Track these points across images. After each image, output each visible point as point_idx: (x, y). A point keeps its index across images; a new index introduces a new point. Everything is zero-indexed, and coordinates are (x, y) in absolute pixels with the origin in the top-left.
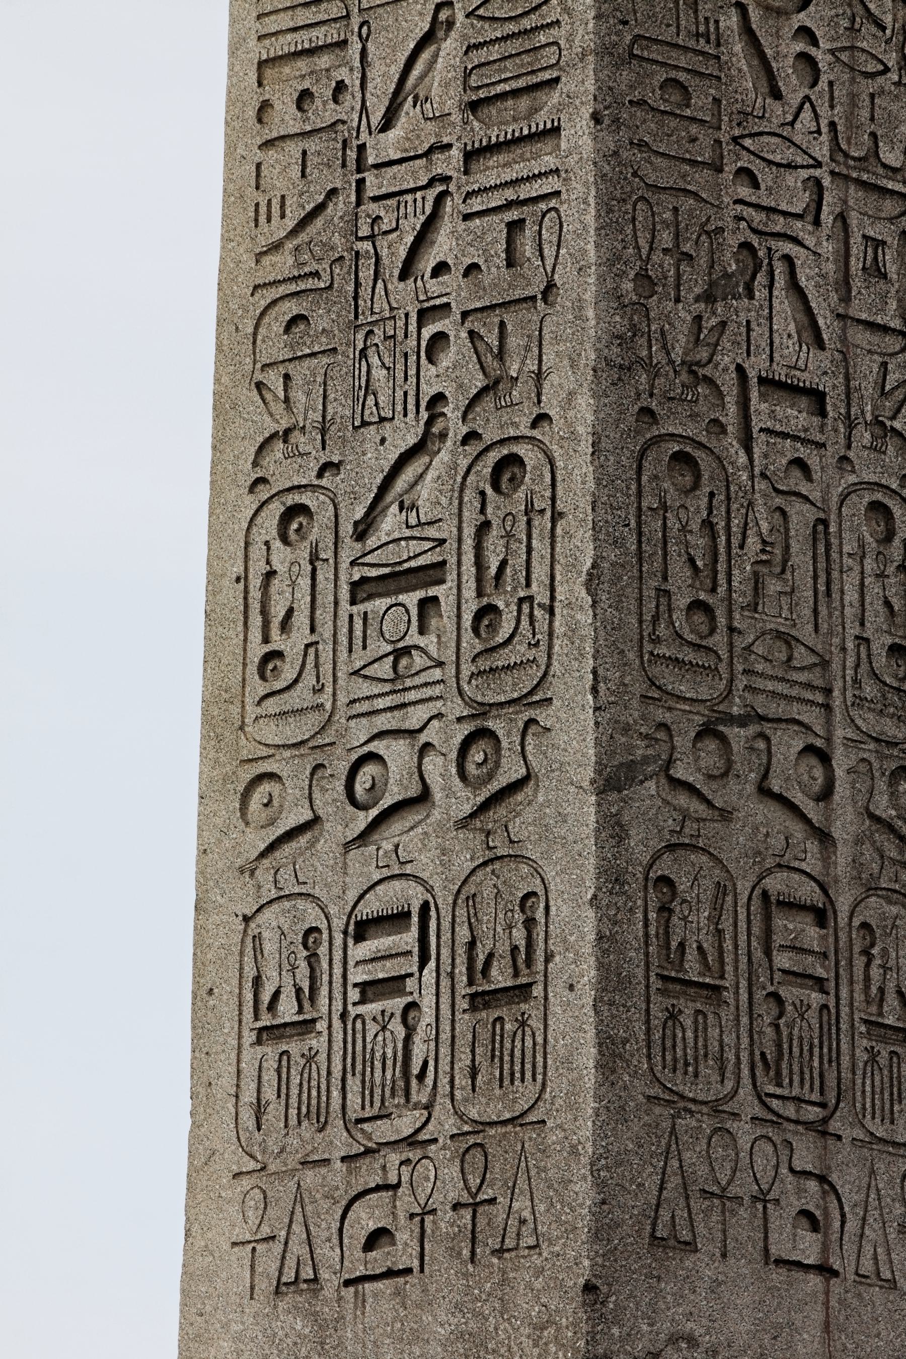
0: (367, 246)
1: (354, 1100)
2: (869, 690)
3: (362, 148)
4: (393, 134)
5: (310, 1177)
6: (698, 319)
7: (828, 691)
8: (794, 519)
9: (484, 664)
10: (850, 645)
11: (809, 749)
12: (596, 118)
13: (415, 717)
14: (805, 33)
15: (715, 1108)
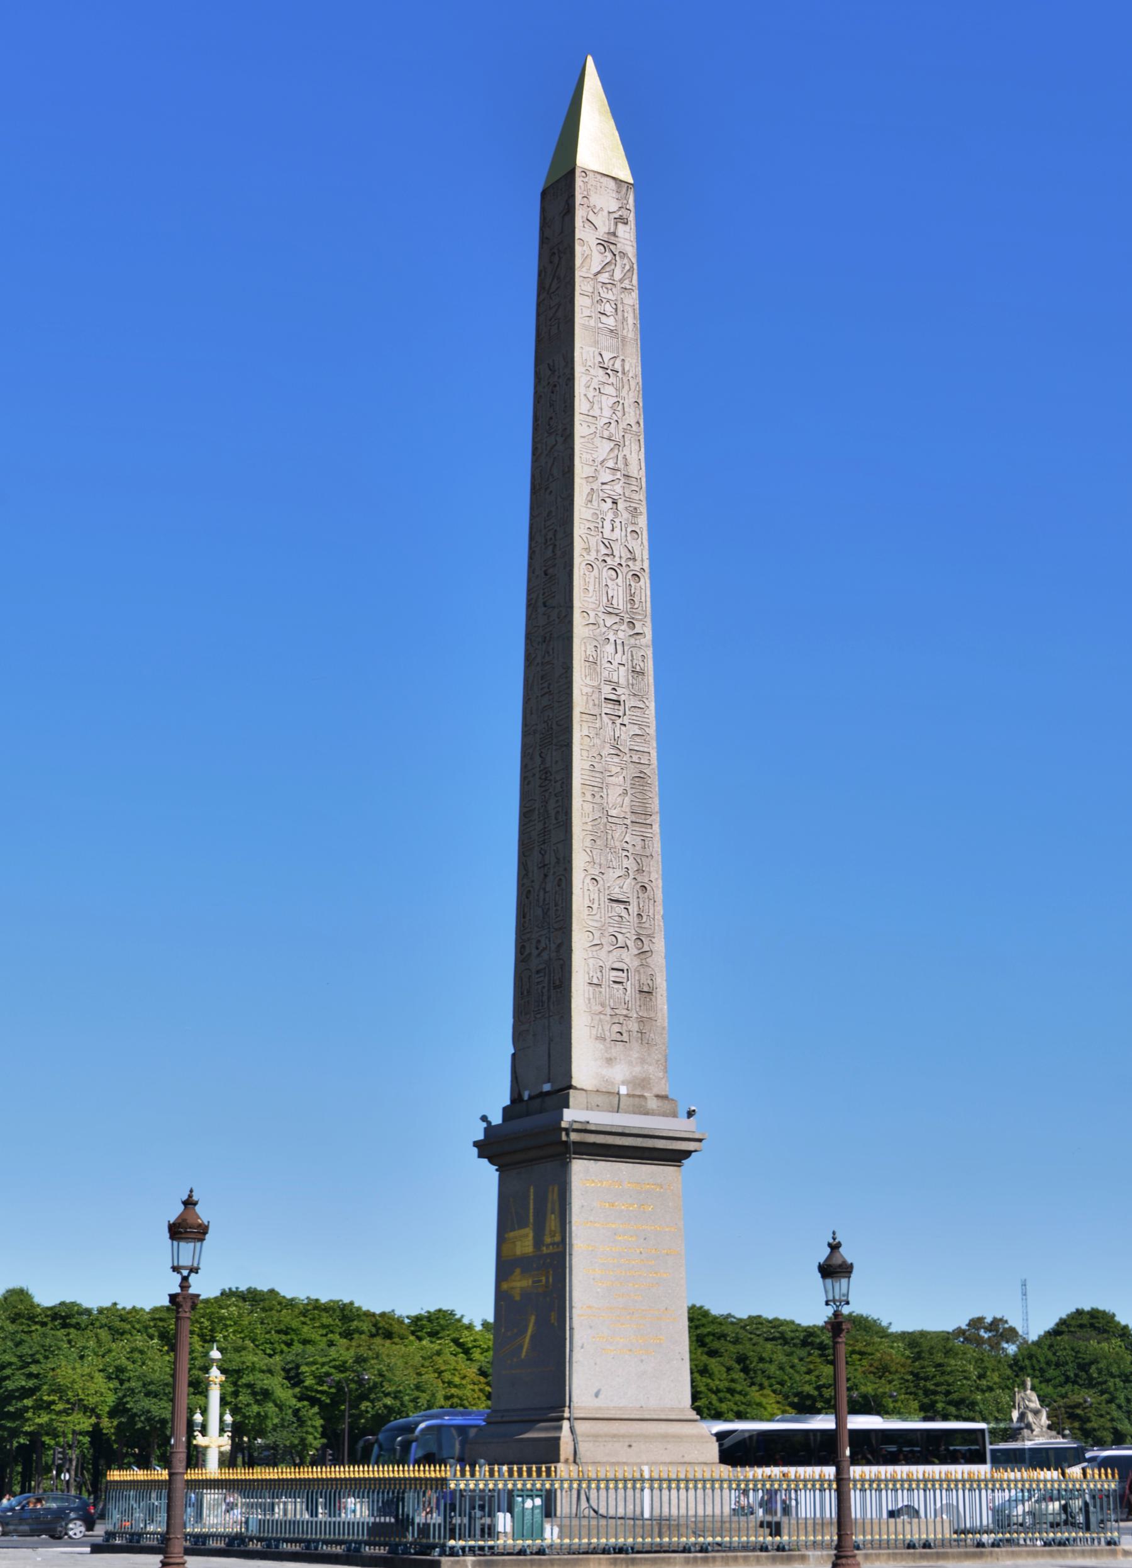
1: (612, 1005)
4: (615, 811)
5: (602, 1016)
13: (624, 931)
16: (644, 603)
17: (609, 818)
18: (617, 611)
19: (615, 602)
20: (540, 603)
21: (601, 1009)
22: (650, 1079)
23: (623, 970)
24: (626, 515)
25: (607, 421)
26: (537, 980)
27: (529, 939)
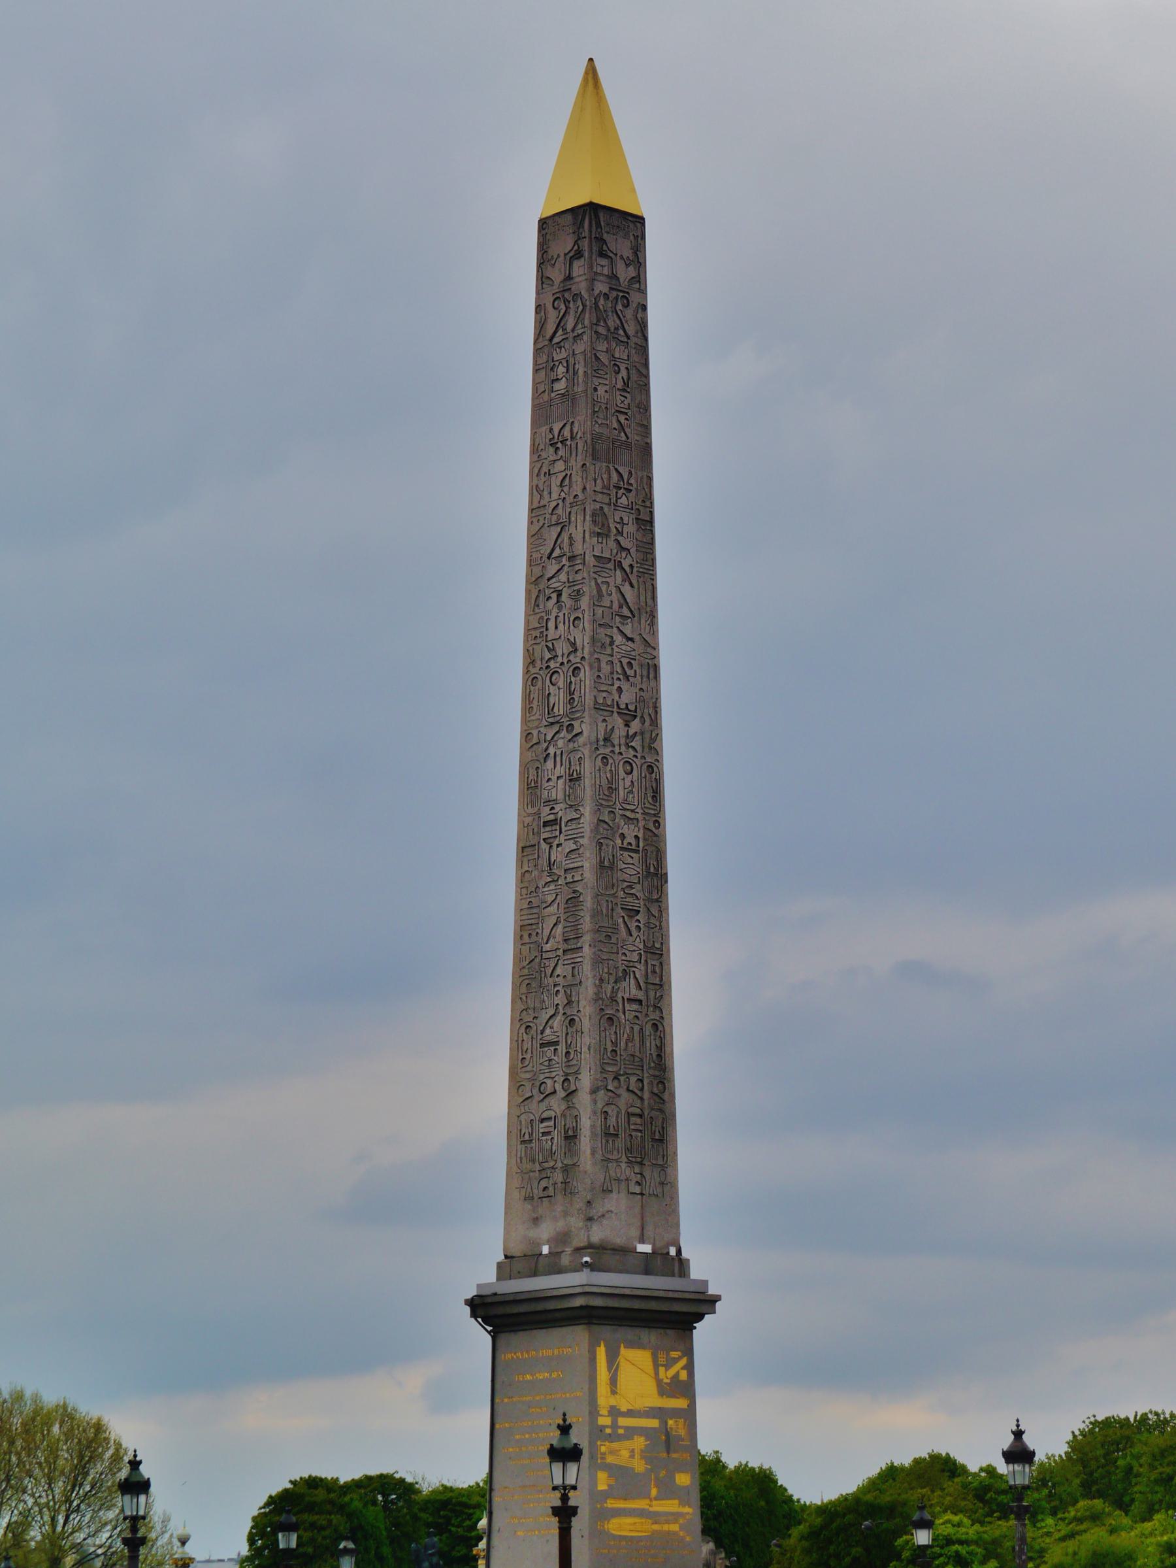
0: (543, 969)
1: (541, 1158)
2: (652, 1065)
3: (542, 947)
4: (548, 945)
5: (532, 1174)
6: (613, 987)
7: (643, 1066)
8: (635, 1029)
9: (567, 1064)
10: (648, 1055)
11: (638, 1079)
12: (590, 945)
13: (554, 1074)
14: (638, 921)
15: (617, 1161)
16: (583, 697)
19: (556, 709)
21: (529, 1166)
22: (571, 1231)
23: (549, 1119)
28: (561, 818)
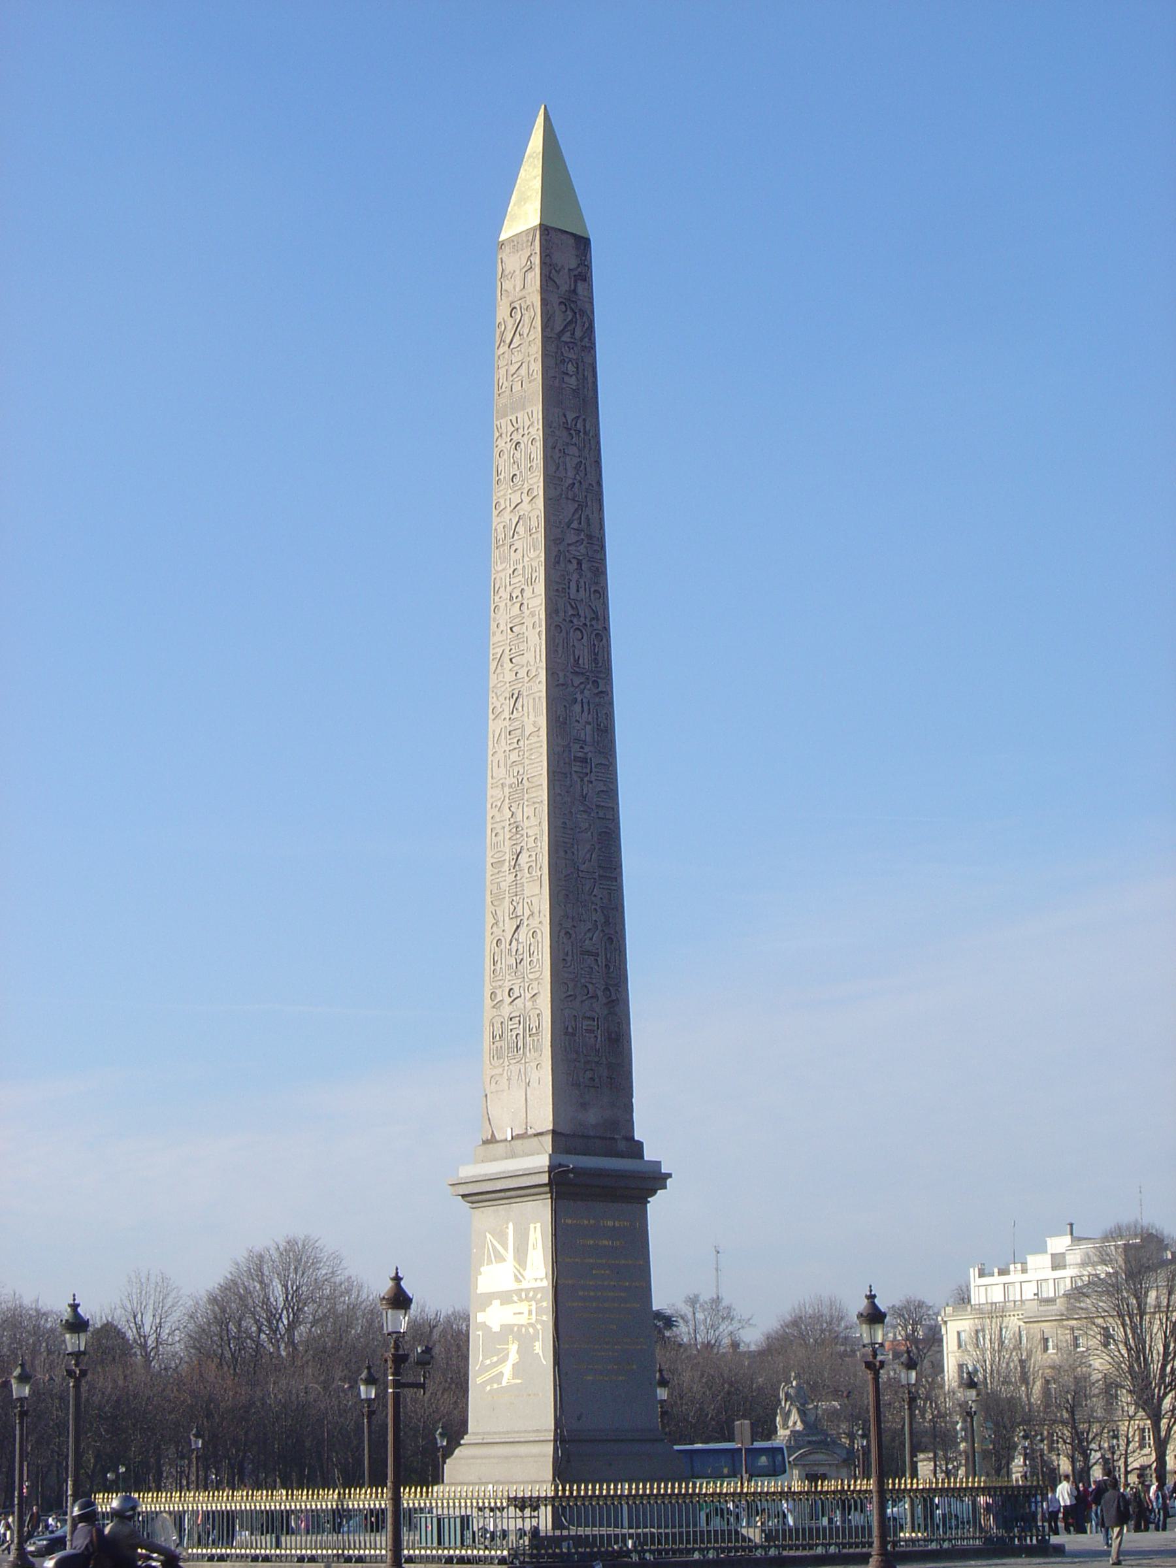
13: (594, 981)
17: (580, 873)
18: (584, 671)
19: (581, 661)
20: (506, 658)
24: (589, 575)
25: (571, 481)
26: (510, 1027)
27: (500, 987)
28: (591, 759)
